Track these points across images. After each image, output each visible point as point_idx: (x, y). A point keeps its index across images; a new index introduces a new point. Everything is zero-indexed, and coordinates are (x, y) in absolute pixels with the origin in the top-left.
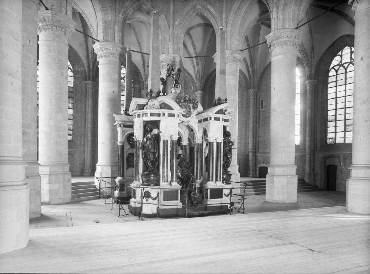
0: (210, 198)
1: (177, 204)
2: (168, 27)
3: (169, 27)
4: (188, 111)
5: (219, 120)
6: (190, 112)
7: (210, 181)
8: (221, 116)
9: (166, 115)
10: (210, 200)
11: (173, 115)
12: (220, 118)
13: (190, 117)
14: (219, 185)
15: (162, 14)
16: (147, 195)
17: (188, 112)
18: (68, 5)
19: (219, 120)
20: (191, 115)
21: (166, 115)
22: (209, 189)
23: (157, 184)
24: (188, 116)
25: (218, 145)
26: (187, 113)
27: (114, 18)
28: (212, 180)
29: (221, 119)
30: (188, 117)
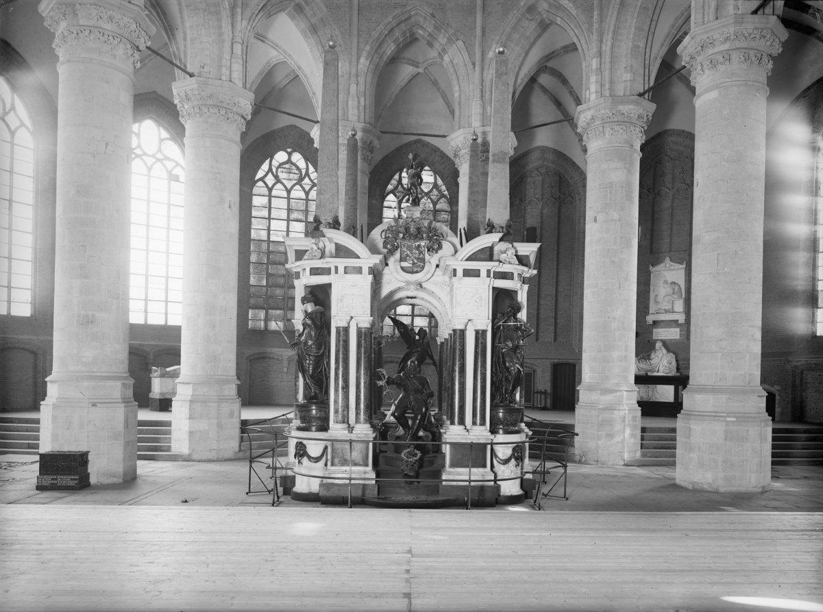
0: (452, 465)
2: (472, 67)
3: (474, 67)
4: (416, 258)
6: (423, 260)
8: (483, 266)
10: (452, 470)
11: (359, 270)
12: (479, 270)
13: (421, 271)
14: (480, 434)
15: (457, 40)
16: (301, 452)
17: (416, 261)
18: (233, 60)
20: (423, 268)
21: (341, 270)
23: (324, 427)
24: (416, 269)
25: (480, 335)
26: (414, 264)
28: (462, 422)
29: (483, 273)
30: (417, 272)
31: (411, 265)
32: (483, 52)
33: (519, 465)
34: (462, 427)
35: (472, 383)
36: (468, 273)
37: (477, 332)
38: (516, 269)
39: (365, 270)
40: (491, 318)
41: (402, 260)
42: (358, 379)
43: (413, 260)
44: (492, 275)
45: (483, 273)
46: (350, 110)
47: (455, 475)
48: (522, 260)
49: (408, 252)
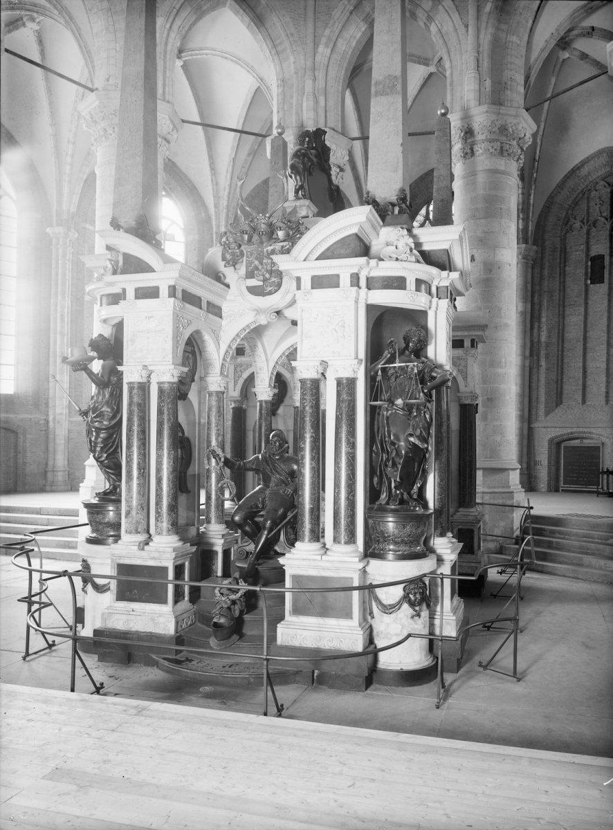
0: (297, 611)
1: (158, 618)
2: (464, 30)
4: (267, 271)
5: (337, 286)
7: (303, 541)
8: (345, 267)
9: (131, 294)
10: (294, 619)
12: (338, 276)
13: (276, 291)
19: (337, 286)
20: (279, 285)
22: (390, 561)
25: (346, 386)
26: (265, 280)
27: (303, 62)
28: (317, 535)
29: (345, 280)
30: (270, 293)
31: (261, 283)
32: (478, 6)
33: (419, 615)
34: (316, 546)
35: (337, 474)
36: (319, 282)
37: (339, 382)
38: (414, 270)
39: (164, 292)
40: (362, 355)
41: (250, 275)
42: (159, 463)
43: (264, 275)
44: (363, 283)
45: (345, 280)
46: (305, 112)
47: (299, 631)
48: (440, 261)
49: (257, 263)
